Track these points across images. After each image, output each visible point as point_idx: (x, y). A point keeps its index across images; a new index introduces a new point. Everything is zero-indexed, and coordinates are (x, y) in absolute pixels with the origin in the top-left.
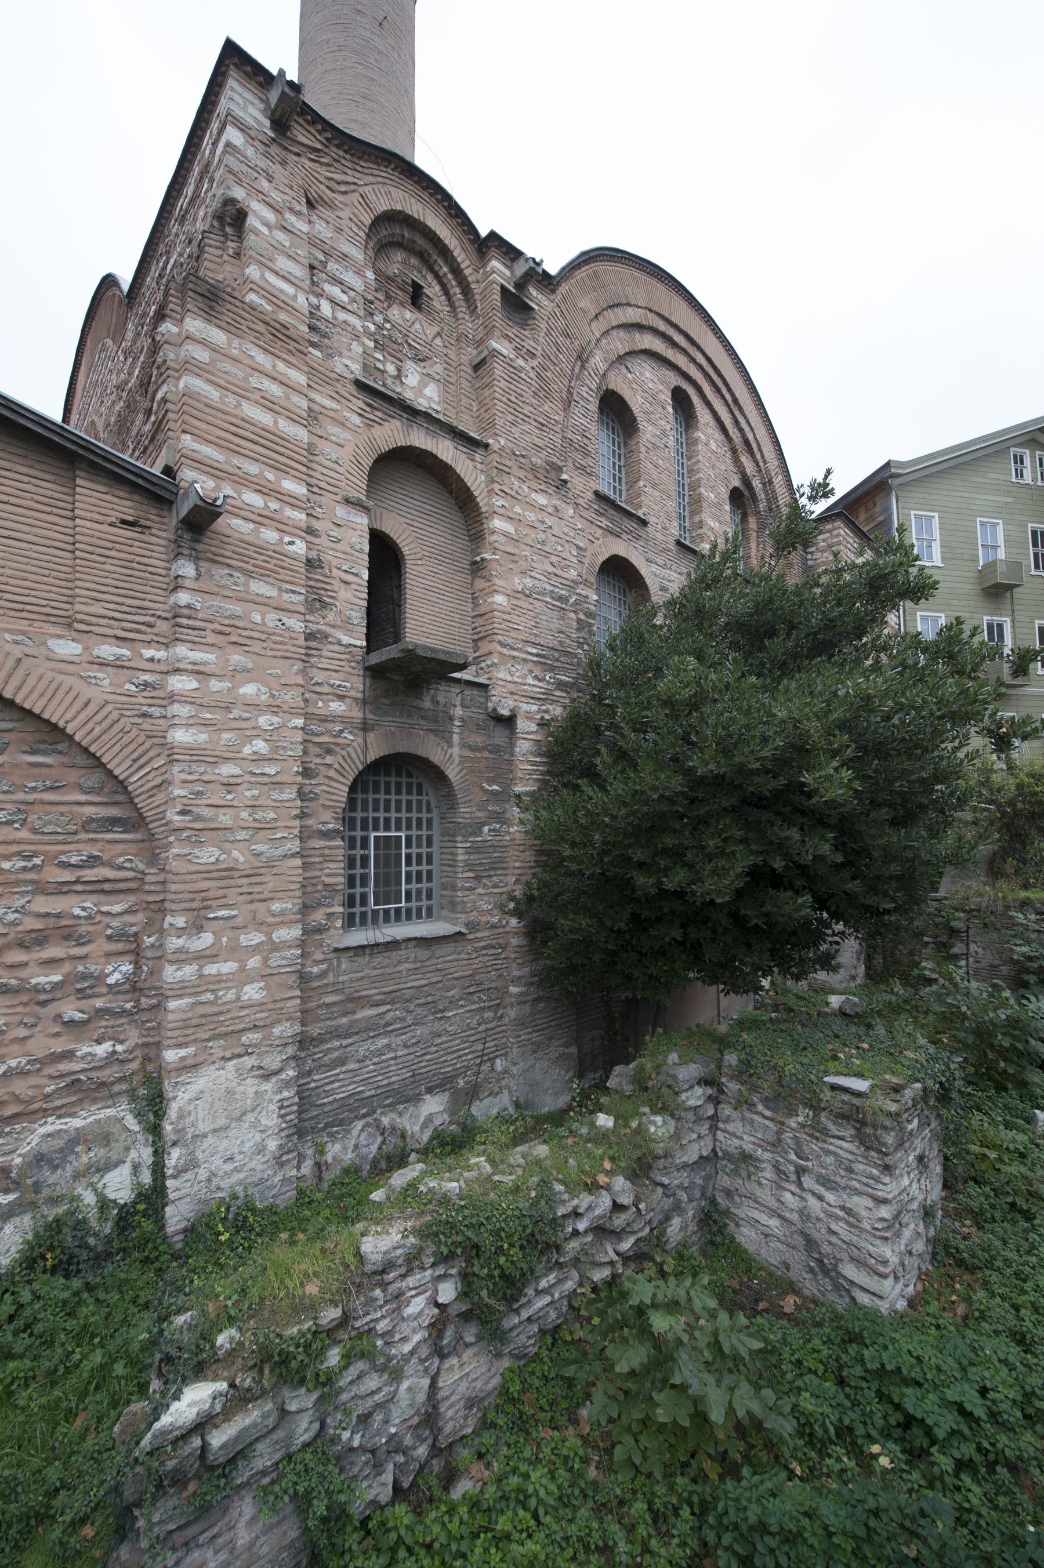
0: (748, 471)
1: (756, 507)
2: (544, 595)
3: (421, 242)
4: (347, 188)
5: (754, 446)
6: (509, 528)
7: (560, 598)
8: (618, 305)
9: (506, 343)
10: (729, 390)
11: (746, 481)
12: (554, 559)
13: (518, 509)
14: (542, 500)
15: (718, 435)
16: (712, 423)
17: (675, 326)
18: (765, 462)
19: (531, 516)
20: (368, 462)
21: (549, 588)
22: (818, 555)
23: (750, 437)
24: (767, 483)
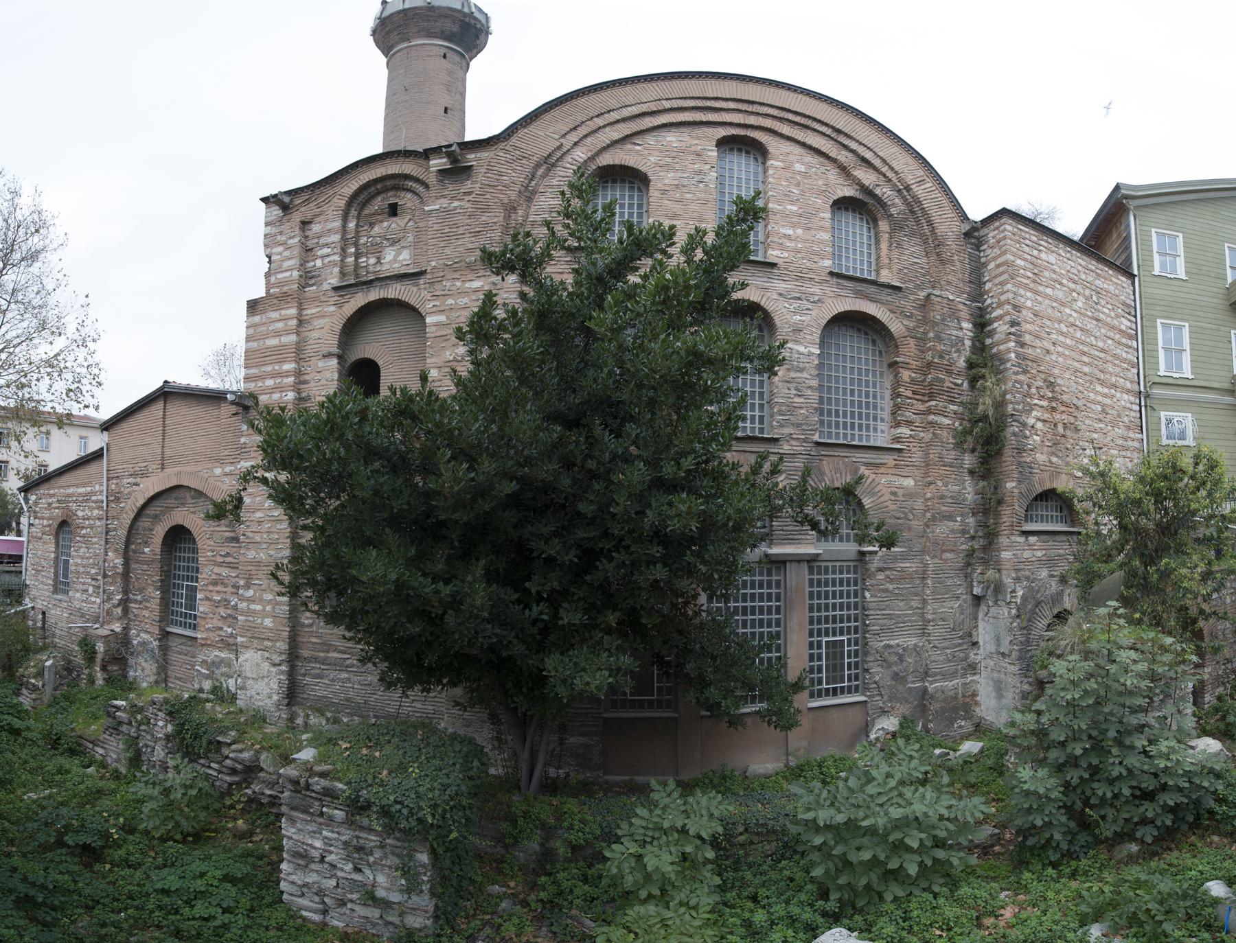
15: (811, 158)
22: (989, 252)
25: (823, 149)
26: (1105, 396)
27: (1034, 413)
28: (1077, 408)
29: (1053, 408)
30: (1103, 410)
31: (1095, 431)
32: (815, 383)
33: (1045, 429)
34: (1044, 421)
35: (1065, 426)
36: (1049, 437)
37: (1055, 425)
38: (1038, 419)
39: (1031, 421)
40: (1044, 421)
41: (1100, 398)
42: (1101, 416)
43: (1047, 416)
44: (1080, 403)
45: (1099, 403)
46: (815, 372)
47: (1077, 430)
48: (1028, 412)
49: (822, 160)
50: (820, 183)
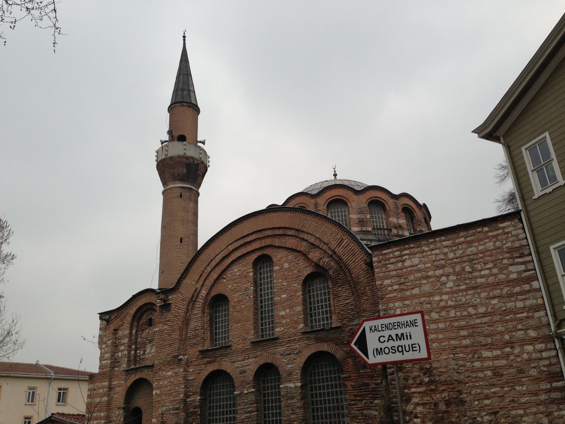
0: (315, 260)
1: (328, 273)
2: (170, 411)
3: (148, 307)
4: (125, 317)
5: (317, 243)
6: (158, 392)
7: (177, 409)
8: (212, 260)
9: (161, 325)
10: (291, 229)
11: (317, 265)
12: (174, 394)
13: (161, 383)
14: (170, 373)
16: (285, 252)
17: (248, 235)
18: (327, 244)
19: (166, 382)
20: (124, 393)
21: (171, 407)
23: (312, 240)
24: (333, 255)
25: (294, 247)
26: (496, 358)
27: (415, 400)
28: (460, 382)
29: (432, 390)
30: (495, 374)
31: (487, 397)
32: (299, 404)
33: (425, 411)
34: (424, 404)
35: (448, 403)
36: (430, 416)
37: (436, 405)
38: (417, 404)
39: (410, 407)
40: (424, 404)
41: (490, 363)
42: (494, 381)
43: (426, 399)
44: (462, 377)
45: (488, 368)
46: (300, 397)
47: (463, 402)
48: (408, 400)
49: (296, 254)
50: (296, 271)
